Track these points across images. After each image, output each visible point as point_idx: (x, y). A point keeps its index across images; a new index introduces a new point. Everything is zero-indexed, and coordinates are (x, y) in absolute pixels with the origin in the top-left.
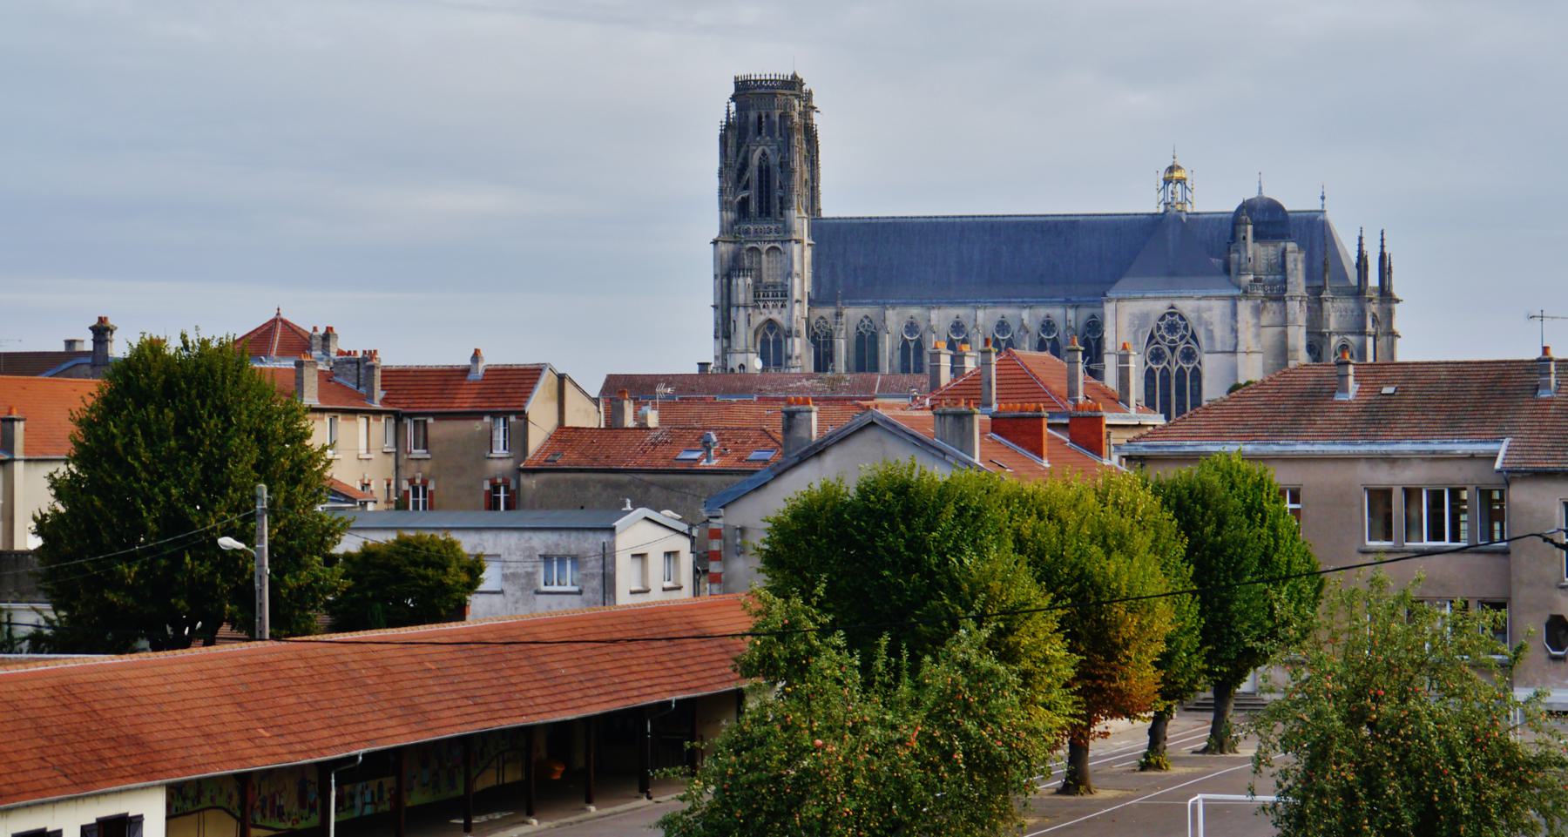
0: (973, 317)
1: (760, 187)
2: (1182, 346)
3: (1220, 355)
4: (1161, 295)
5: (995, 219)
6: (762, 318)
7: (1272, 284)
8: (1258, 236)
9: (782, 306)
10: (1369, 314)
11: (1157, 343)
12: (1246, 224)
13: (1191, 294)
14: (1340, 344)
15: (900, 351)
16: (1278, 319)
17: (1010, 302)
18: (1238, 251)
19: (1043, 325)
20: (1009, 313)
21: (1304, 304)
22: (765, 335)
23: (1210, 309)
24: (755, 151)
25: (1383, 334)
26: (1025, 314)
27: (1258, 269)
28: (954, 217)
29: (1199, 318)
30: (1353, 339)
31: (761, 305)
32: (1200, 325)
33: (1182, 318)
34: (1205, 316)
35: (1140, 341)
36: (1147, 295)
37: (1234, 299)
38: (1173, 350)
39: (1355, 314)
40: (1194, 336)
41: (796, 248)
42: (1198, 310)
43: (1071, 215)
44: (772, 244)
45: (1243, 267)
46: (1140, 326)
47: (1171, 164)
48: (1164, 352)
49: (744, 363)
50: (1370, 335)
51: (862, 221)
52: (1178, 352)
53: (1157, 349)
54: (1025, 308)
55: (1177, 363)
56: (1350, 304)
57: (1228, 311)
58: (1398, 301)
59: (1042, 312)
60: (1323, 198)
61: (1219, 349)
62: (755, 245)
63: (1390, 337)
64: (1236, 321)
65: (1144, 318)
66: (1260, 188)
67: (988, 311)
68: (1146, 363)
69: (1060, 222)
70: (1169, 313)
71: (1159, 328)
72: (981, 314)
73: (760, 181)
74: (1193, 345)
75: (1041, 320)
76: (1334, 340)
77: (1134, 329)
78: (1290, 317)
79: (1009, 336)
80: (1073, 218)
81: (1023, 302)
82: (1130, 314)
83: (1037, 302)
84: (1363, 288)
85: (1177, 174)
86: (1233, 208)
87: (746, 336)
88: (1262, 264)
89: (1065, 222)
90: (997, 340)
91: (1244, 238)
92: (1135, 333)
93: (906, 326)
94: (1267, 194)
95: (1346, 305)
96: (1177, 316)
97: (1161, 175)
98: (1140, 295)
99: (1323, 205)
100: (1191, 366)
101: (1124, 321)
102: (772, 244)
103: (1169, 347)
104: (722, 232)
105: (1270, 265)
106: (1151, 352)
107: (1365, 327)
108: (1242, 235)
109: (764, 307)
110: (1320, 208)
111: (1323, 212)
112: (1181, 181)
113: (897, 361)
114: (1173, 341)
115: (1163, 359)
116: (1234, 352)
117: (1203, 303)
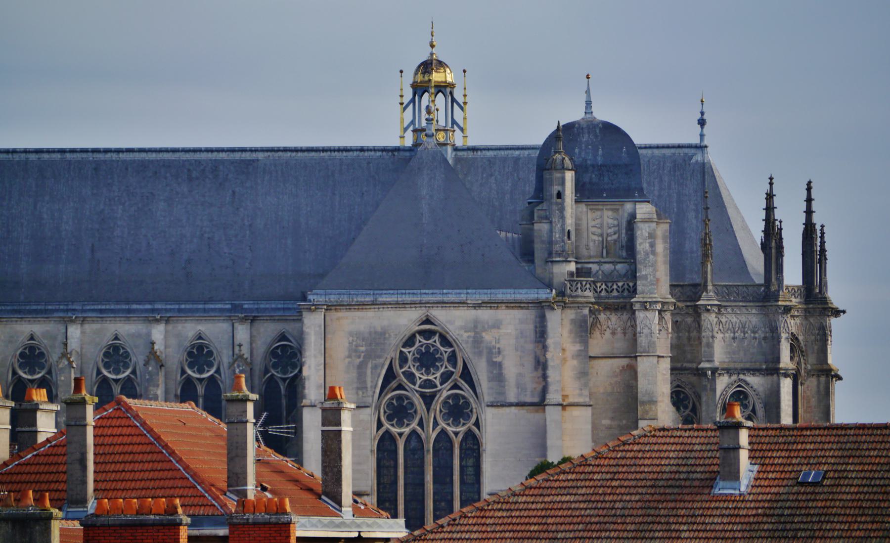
0: (61, 338)
2: (445, 394)
3: (513, 408)
4: (408, 298)
5: (101, 156)
7: (609, 279)
8: (584, 192)
10: (784, 336)
11: (400, 387)
12: (563, 168)
13: (463, 297)
14: (730, 392)
16: (620, 345)
17: (129, 311)
18: (548, 219)
19: (190, 354)
21: (668, 316)
23: (497, 325)
25: (809, 374)
26: (158, 333)
27: (584, 252)
28: (26, 151)
29: (477, 341)
30: (755, 381)
32: (480, 354)
33: (445, 341)
34: (487, 337)
35: (369, 384)
36: (381, 299)
37: (541, 307)
38: (428, 400)
39: (760, 334)
40: (466, 375)
42: (476, 328)
43: (243, 150)
45: (557, 248)
46: (369, 356)
47: (425, 57)
48: (412, 404)
50: (786, 375)
52: (437, 405)
53: (400, 398)
54: (157, 321)
55: (436, 424)
56: (752, 317)
57: (530, 328)
58: (837, 313)
59: (189, 329)
60: (702, 123)
61: (512, 398)
63: (823, 379)
64: (545, 348)
65: (376, 339)
66: (589, 104)
67: (88, 327)
68: (380, 425)
69: (222, 161)
70: (421, 333)
71: (403, 359)
72: (75, 332)
74: (466, 391)
75: (187, 344)
76: (722, 383)
77: (358, 361)
78: (642, 341)
79: (127, 373)
80: (247, 156)
81: (153, 311)
82: (351, 334)
83: (180, 310)
84: (773, 288)
85: (437, 77)
86: (538, 138)
88: (591, 244)
89: (232, 162)
90: (105, 379)
91: (559, 195)
92: (361, 367)
94: (601, 114)
95: (743, 319)
96: (437, 338)
97: (409, 78)
98: (369, 299)
99: (702, 136)
100: (462, 429)
101: (340, 345)
103: (423, 395)
105: (606, 247)
106: (389, 405)
107: (778, 360)
108: (556, 188)
110: (696, 140)
111: (701, 148)
112: (443, 88)
113: (370, 482)
114: (428, 384)
115: (411, 417)
116: (541, 404)
117: (485, 314)
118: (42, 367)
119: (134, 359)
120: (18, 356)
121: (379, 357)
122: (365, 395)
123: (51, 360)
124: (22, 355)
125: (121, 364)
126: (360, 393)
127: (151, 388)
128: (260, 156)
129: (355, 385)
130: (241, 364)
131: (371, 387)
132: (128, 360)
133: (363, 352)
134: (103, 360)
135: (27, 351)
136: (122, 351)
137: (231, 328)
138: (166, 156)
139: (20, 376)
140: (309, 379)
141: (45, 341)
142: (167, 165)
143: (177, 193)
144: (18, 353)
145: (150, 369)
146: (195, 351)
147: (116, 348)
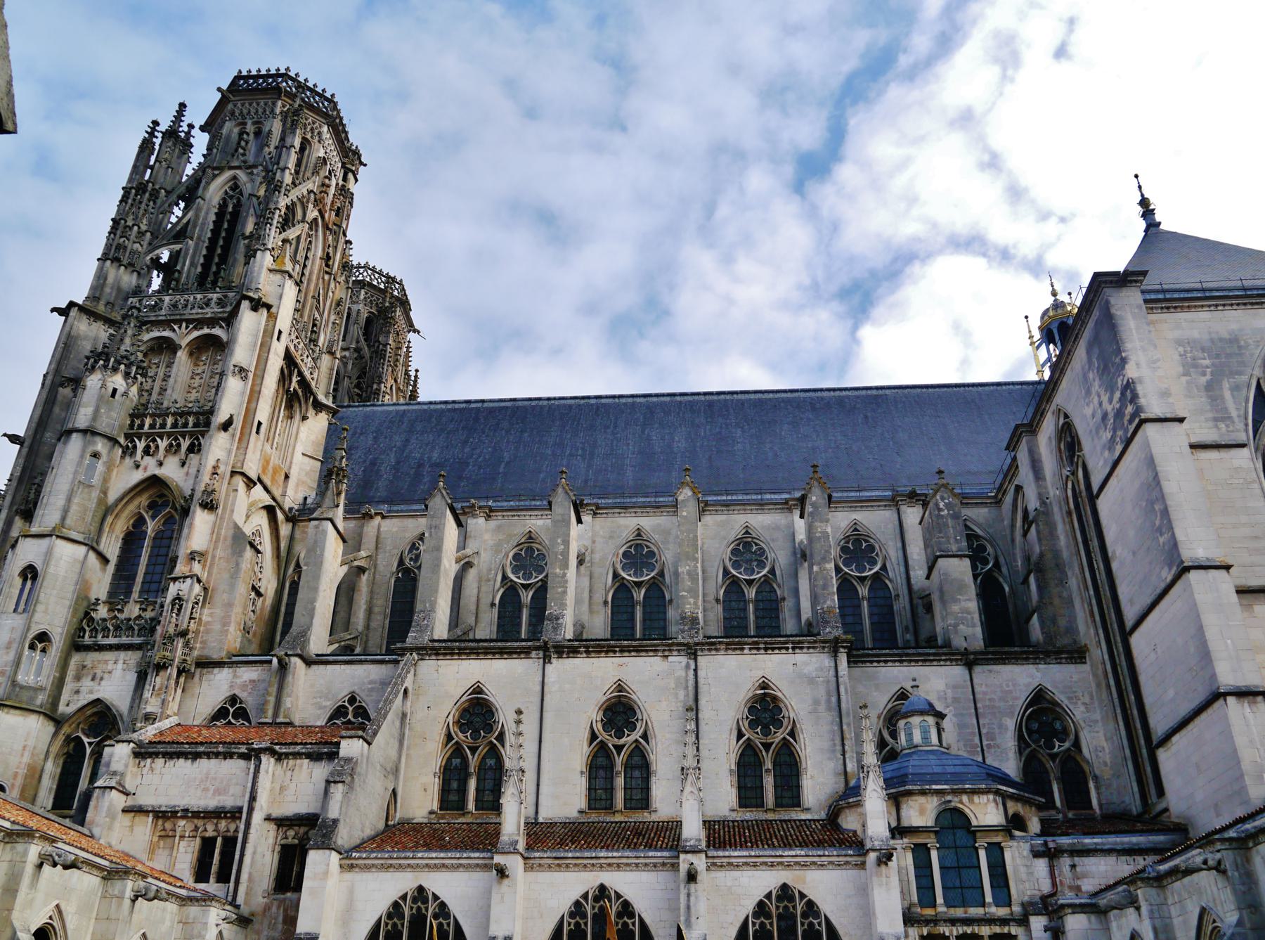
1: (213, 241)
6: (138, 476)
9: (191, 450)
15: (496, 610)
20: (761, 522)
22: (140, 521)
24: (215, 176)
31: (141, 445)
41: (249, 322)
44: (206, 331)
49: (39, 566)
51: (449, 406)
62: (167, 333)
73: (216, 232)
77: (1203, 380)
87: (69, 500)
93: (516, 557)
102: (206, 331)
104: (94, 296)
109: (147, 452)
118: (651, 567)
119: (771, 556)
120: (620, 556)
121: (1240, 373)
122: (1231, 428)
123: (663, 558)
124: (625, 554)
125: (755, 563)
126: (1222, 425)
127: (817, 524)
128: (888, 392)
129: (1210, 415)
130: (946, 495)
131: (1239, 416)
132: (763, 558)
133: (1207, 367)
134: (730, 559)
135: (632, 550)
136: (755, 548)
137: (896, 516)
138: (783, 395)
139: (623, 578)
140: (1141, 382)
141: (656, 537)
142: (788, 401)
143: (801, 419)
144: (621, 552)
145: (814, 498)
146: (850, 545)
147: (747, 545)
